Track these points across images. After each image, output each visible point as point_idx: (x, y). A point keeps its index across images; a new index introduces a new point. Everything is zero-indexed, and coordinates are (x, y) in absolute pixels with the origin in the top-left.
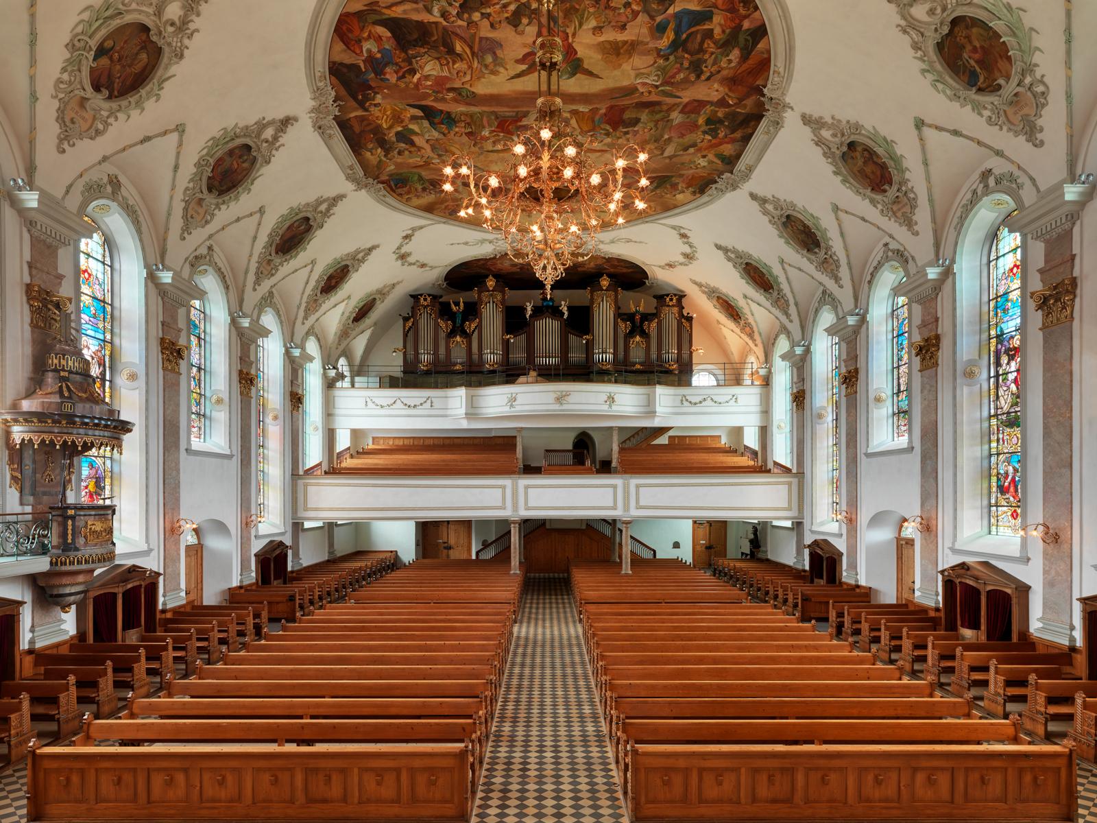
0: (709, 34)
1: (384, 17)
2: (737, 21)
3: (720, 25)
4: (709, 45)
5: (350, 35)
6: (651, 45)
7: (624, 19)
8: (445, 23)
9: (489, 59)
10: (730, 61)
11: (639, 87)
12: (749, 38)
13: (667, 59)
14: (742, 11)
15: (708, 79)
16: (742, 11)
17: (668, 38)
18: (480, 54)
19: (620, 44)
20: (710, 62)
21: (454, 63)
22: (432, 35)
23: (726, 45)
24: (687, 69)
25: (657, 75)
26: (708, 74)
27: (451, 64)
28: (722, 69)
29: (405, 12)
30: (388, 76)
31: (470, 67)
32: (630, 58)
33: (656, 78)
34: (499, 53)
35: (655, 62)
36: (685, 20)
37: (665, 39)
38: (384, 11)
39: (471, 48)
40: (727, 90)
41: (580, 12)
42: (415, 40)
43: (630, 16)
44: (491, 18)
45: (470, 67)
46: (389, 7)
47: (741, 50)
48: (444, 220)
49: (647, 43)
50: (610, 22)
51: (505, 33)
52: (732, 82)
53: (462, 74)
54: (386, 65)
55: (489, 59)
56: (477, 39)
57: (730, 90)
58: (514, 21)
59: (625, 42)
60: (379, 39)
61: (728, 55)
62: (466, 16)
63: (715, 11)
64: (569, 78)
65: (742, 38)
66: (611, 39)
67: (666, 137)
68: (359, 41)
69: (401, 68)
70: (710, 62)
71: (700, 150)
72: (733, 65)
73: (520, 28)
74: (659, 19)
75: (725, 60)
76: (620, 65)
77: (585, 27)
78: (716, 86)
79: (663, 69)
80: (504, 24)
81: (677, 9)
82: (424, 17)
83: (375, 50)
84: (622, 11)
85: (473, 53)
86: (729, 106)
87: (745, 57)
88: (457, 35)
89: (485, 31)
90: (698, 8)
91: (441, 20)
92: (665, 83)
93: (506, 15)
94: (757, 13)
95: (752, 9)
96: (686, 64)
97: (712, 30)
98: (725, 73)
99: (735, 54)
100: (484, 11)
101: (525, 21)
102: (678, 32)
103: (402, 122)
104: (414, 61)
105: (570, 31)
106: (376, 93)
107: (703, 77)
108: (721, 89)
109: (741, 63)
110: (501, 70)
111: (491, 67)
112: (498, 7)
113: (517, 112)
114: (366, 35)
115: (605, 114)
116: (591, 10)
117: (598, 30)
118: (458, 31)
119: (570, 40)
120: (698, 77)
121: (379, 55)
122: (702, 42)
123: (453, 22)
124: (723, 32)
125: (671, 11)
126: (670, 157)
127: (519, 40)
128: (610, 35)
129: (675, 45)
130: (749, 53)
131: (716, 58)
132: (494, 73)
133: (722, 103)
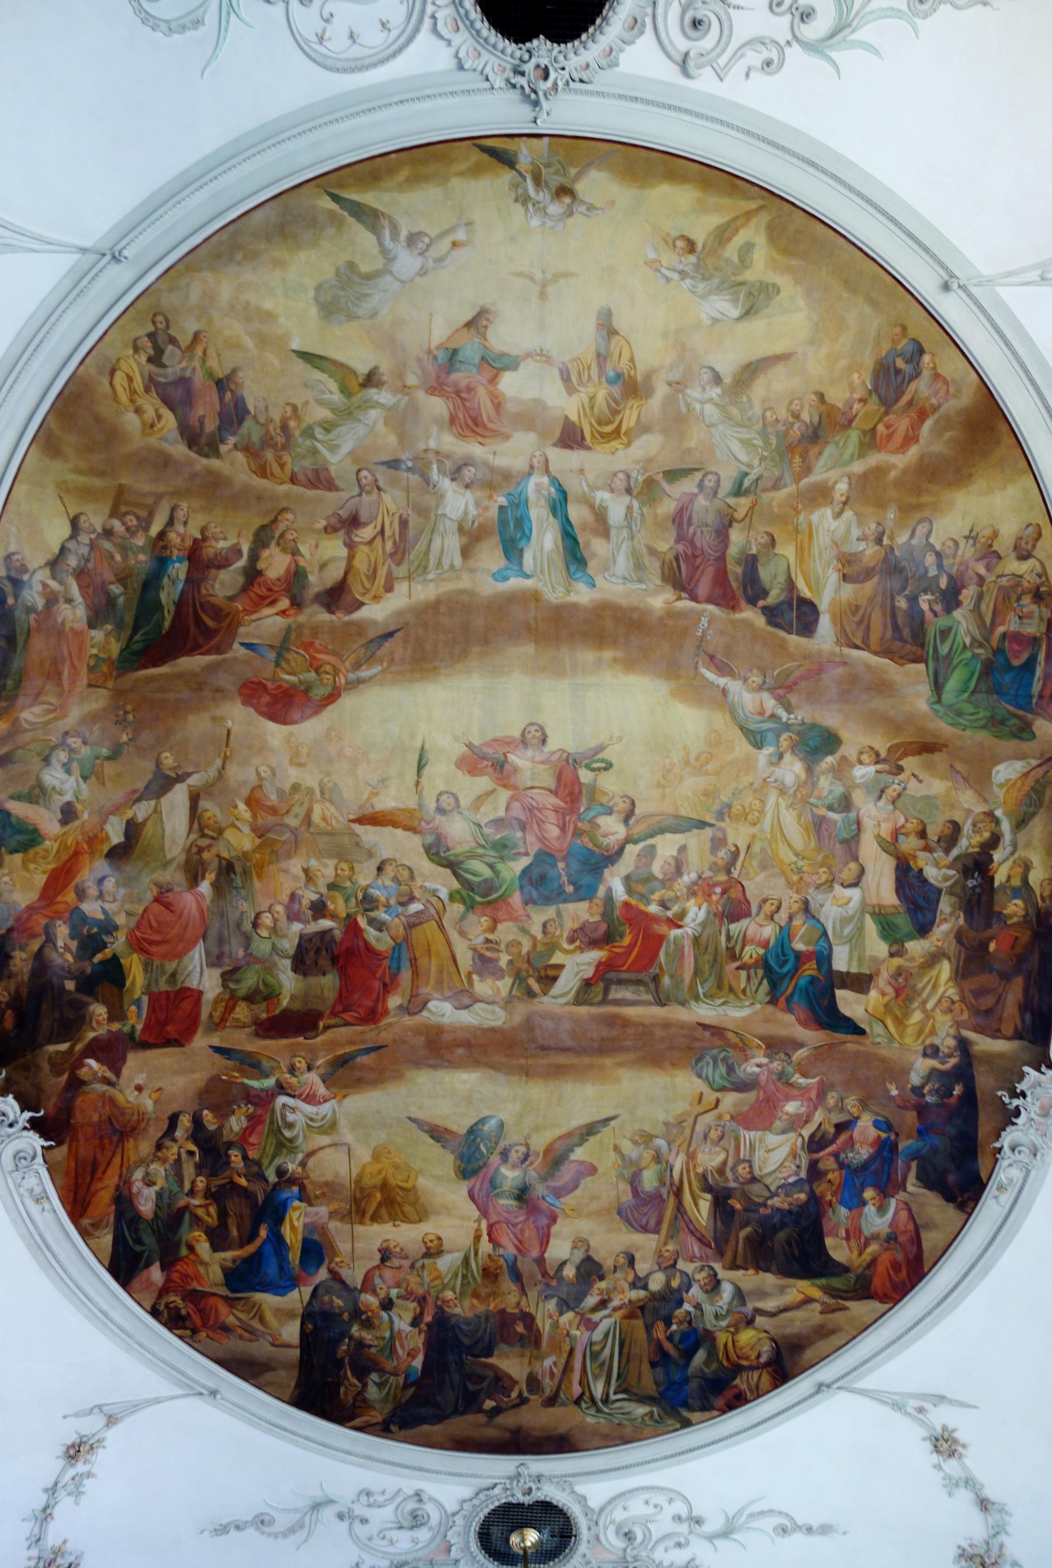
0: (218, 1240)
1: (823, 1281)
2: (175, 1276)
3: (203, 1263)
4: (210, 1215)
5: (900, 1257)
6: (323, 1210)
7: (388, 1274)
8: (717, 1266)
9: (649, 1180)
10: (149, 1183)
11: (322, 1090)
12: (138, 1248)
13: (281, 1172)
14: (175, 1299)
15: (173, 1120)
16: (175, 1299)
17: (293, 1228)
18: (664, 1191)
19: (384, 1212)
20: (189, 1170)
21: (721, 1170)
22: (747, 1238)
23: (171, 1219)
24: (230, 1145)
25: (290, 1126)
26: (178, 1134)
27: (730, 1164)
28: (156, 1158)
29: (782, 1290)
30: (873, 1133)
31: (691, 1156)
32: (360, 1176)
33: (291, 1117)
34: (627, 1197)
35: (303, 1164)
36: (271, 1269)
37: (299, 1224)
38: (817, 1294)
39: (680, 1207)
40: (120, 1098)
41: (470, 1290)
42: (783, 1225)
43: (377, 1280)
44: (631, 1278)
45: (691, 1156)
46: (808, 1300)
47: (138, 1217)
48: (951, 310)
49: (332, 1215)
50: (412, 1266)
51: (610, 1241)
52: (120, 1128)
53: (714, 1135)
54: (865, 1166)
55: (649, 1180)
56: (665, 1226)
57: (112, 1101)
58: (591, 1269)
59: (375, 1218)
60: (853, 1233)
61: (159, 1195)
62: (675, 1284)
63: (224, 1291)
64: (482, 1121)
65: (150, 1240)
66: (404, 1227)
67: (205, 888)
68: (891, 1238)
69: (836, 1155)
70: (189, 1170)
71: (94, 840)
72: (138, 1174)
73: (579, 1256)
74: (323, 1274)
75: (160, 1183)
76: (376, 1156)
77: (457, 1257)
78: (148, 1103)
79: (284, 1146)
80: (608, 1264)
81: (294, 1294)
82: (749, 1279)
83: (870, 1209)
84: (394, 1292)
85: (678, 1193)
86: (96, 1049)
87: (123, 1201)
88: (702, 1240)
89: (646, 1245)
90: (259, 1296)
91: (722, 1274)
92: (263, 1100)
93: (603, 1285)
94: (148, 1305)
95: (162, 1308)
96: (235, 1156)
97: (215, 1248)
98: (145, 1147)
99: (146, 1204)
100: (642, 1293)
101: (569, 1272)
102: (277, 1240)
103: (899, 972)
104: (803, 1175)
105: (485, 1246)
106: (917, 1091)
107: (185, 1122)
108: (132, 1096)
109: (126, 1182)
110: (627, 1147)
111: (648, 1155)
112: (616, 1302)
113: (604, 1001)
114: (873, 1248)
115: (387, 988)
116: (449, 1294)
117: (433, 1250)
118: (696, 1248)
119: (484, 1225)
120: (197, 1121)
121: (869, 1194)
122: (223, 1215)
123: (702, 1268)
124: (191, 1249)
125: (307, 1291)
126: (163, 783)
127: (584, 1226)
128: (405, 1235)
129: (272, 1211)
130: (119, 1216)
131: (180, 1181)
132: (645, 1139)
133: (112, 1051)
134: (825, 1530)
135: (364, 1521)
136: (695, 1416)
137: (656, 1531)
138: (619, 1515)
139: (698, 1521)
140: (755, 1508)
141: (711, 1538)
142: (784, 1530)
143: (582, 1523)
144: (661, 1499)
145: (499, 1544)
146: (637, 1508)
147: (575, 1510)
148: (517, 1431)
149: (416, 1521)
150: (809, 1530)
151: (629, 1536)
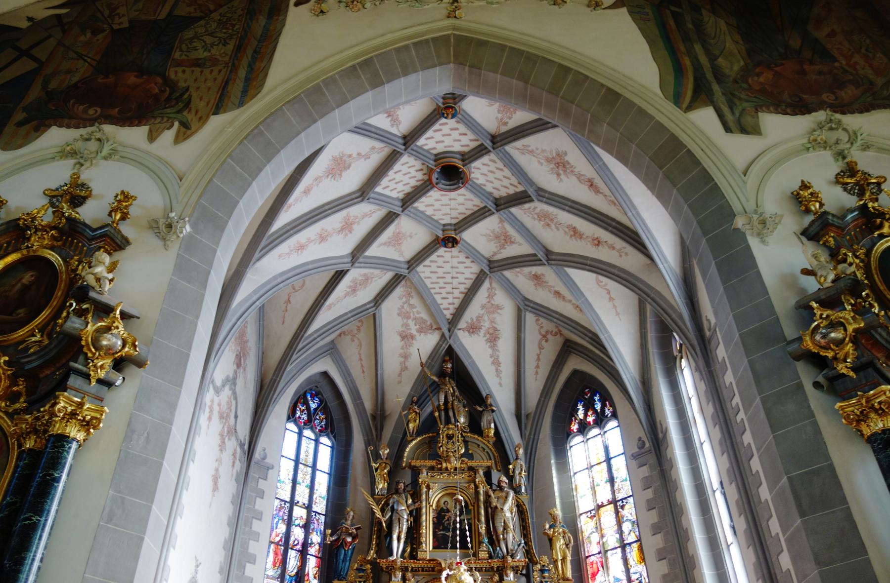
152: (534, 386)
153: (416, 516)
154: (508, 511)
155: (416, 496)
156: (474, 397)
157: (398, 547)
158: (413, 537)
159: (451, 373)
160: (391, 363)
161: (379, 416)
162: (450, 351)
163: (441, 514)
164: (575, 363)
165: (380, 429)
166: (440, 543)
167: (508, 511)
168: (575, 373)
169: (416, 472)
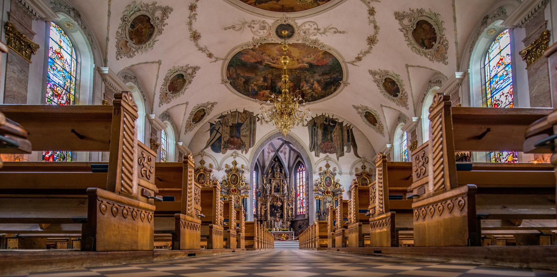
134: (344, 32)
135: (253, 28)
136: (321, 3)
137: (311, 31)
138: (303, 28)
139: (319, 30)
140: (330, 27)
141: (321, 34)
142: (335, 32)
143: (296, 29)
144: (311, 24)
145: (280, 34)
146: (307, 26)
147: (295, 26)
148: (283, 6)
149: (264, 28)
150: (340, 32)
151: (305, 33)
152: (292, 162)
153: (271, 187)
154: (286, 187)
155: (270, 183)
156: (281, 166)
157: (268, 192)
158: (271, 191)
159: (277, 159)
160: (266, 157)
161: (263, 167)
162: (277, 156)
163: (275, 187)
164: (299, 159)
165: (264, 169)
166: (275, 192)
167: (286, 187)
168: (299, 161)
169: (270, 180)
